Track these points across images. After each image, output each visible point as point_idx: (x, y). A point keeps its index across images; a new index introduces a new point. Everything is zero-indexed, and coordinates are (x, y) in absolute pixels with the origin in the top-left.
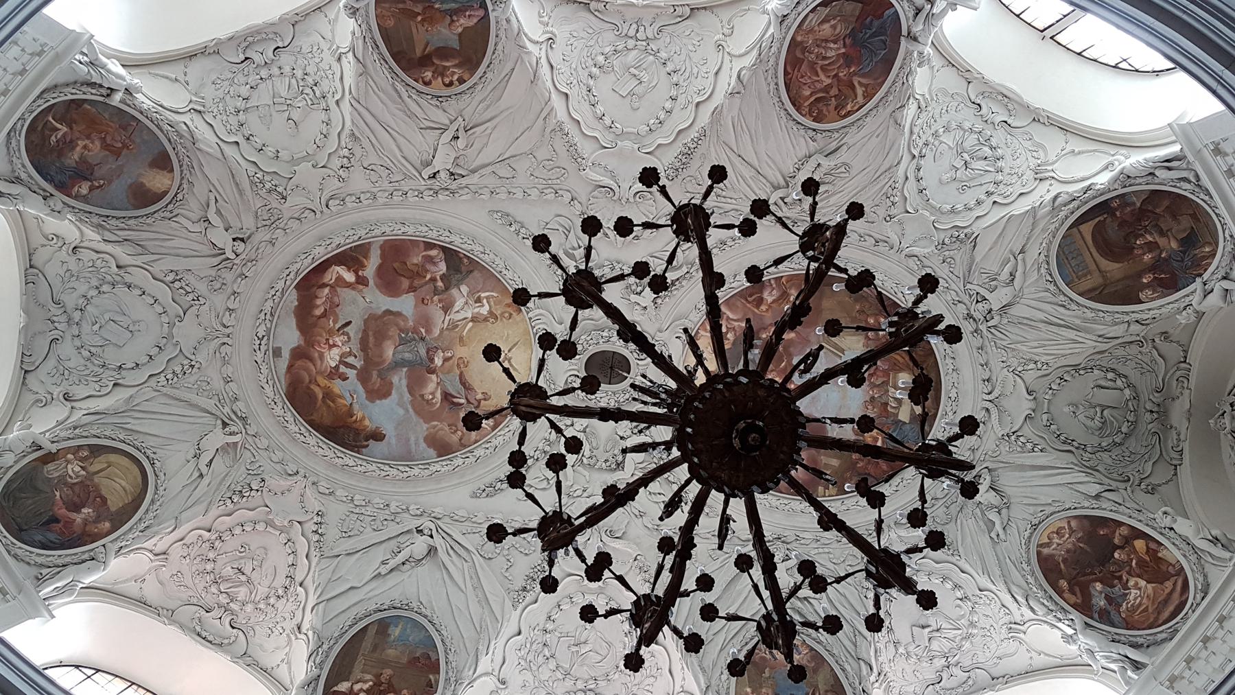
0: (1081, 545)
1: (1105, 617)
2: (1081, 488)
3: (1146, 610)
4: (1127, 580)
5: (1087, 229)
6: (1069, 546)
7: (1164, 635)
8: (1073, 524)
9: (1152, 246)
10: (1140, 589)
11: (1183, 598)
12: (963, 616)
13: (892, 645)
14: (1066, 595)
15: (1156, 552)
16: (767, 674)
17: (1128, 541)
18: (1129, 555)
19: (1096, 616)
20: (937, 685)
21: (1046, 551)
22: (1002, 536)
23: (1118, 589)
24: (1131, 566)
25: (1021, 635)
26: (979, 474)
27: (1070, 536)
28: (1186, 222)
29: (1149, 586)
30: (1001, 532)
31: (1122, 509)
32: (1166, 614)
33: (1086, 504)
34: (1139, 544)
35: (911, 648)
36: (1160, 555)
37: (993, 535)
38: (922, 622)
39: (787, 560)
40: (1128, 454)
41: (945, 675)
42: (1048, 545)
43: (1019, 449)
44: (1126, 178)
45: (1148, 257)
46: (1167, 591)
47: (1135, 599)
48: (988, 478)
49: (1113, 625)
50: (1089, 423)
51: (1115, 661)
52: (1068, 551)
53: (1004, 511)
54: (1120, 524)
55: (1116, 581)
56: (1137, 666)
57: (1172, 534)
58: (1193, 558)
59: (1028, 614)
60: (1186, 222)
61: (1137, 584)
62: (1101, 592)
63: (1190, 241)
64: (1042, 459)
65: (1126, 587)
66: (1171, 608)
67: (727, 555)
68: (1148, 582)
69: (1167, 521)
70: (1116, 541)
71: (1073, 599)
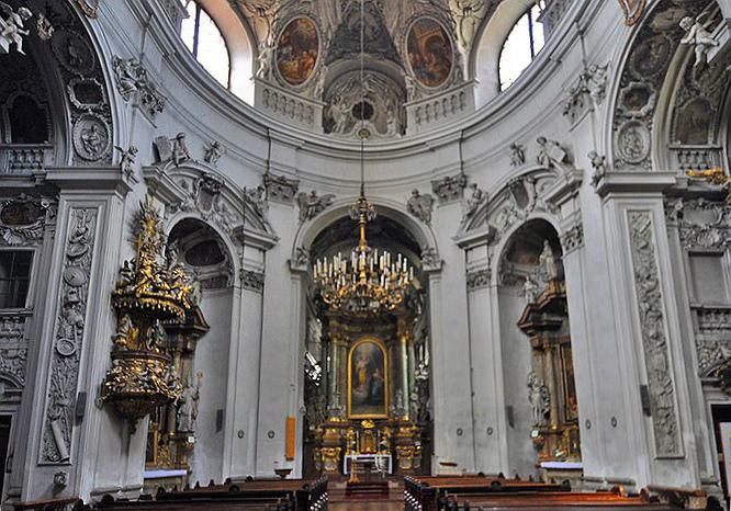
1: (279, 55)
5: (441, 34)
9: (430, 61)
17: (311, 55)
28: (438, 75)
32: (290, 80)
34: (311, 60)
44: (458, 56)
45: (426, 58)
56: (266, 75)
60: (438, 75)
63: (431, 76)
64: (339, 9)
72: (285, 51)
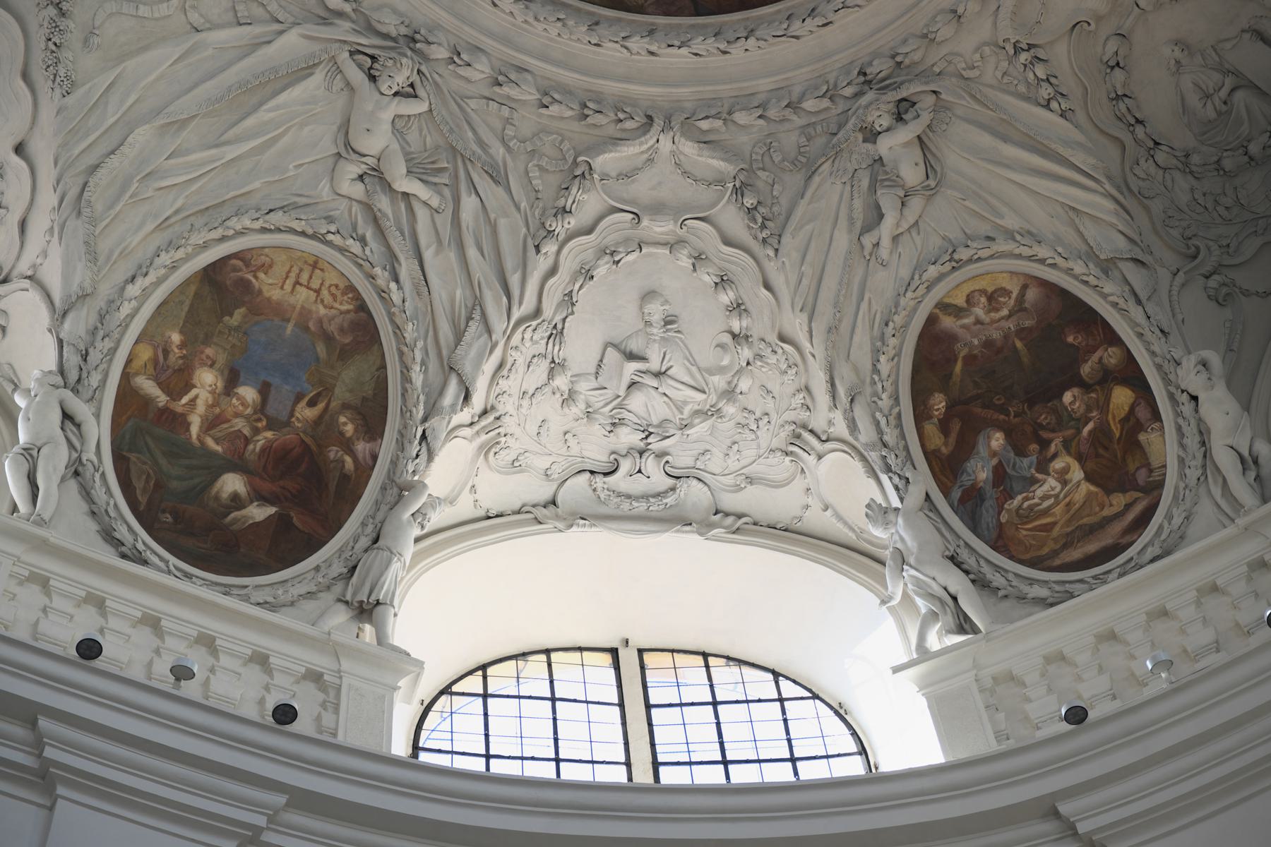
0: (1019, 344)
2: (1091, 231)
3: (1048, 528)
4: (1055, 456)
6: (996, 335)
7: (1042, 592)
8: (1032, 294)
10: (1064, 483)
11: (1124, 541)
12: (721, 370)
13: (544, 365)
14: (931, 428)
15: (1139, 427)
16: (239, 314)
17: (1107, 378)
18: (1089, 409)
19: (956, 494)
20: (599, 480)
21: (947, 322)
22: (884, 252)
23: (1026, 464)
24: (1079, 431)
25: (811, 459)
26: (914, 99)
27: (1009, 316)
29: (1086, 487)
30: (886, 242)
31: (1137, 313)
32: (1075, 554)
33: (1079, 268)
34: (1122, 397)
35: (583, 386)
36: (1142, 437)
37: (868, 241)
38: (634, 346)
39: (408, 96)
40: (1228, 201)
41: (625, 466)
42: (957, 312)
43: (1022, 88)
46: (1107, 512)
47: (1045, 497)
48: (926, 118)
49: (975, 529)
50: (1194, 100)
51: (931, 596)
52: (988, 344)
53: (916, 203)
54: (1113, 338)
55: (1034, 447)
57: (1187, 409)
58: (1193, 474)
59: (841, 429)
61: (1066, 470)
62: (994, 454)
65: (1043, 467)
66: (1092, 547)
67: (277, 27)
68: (1089, 478)
69: (1190, 378)
70: (1086, 369)
71: (936, 440)
72: (980, 471)
